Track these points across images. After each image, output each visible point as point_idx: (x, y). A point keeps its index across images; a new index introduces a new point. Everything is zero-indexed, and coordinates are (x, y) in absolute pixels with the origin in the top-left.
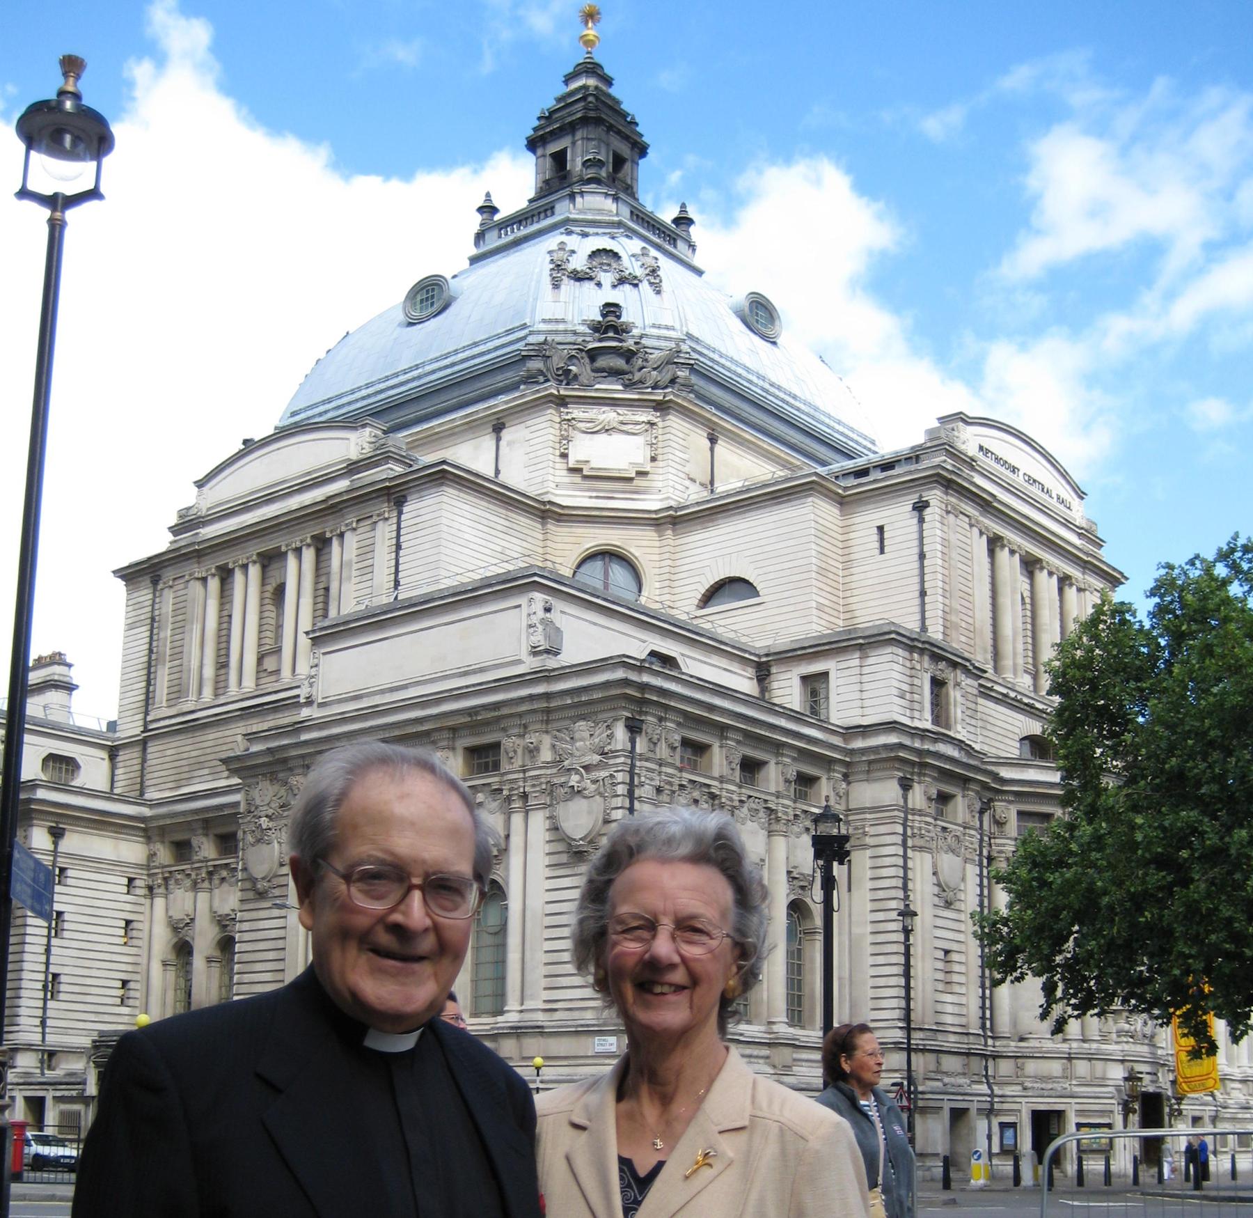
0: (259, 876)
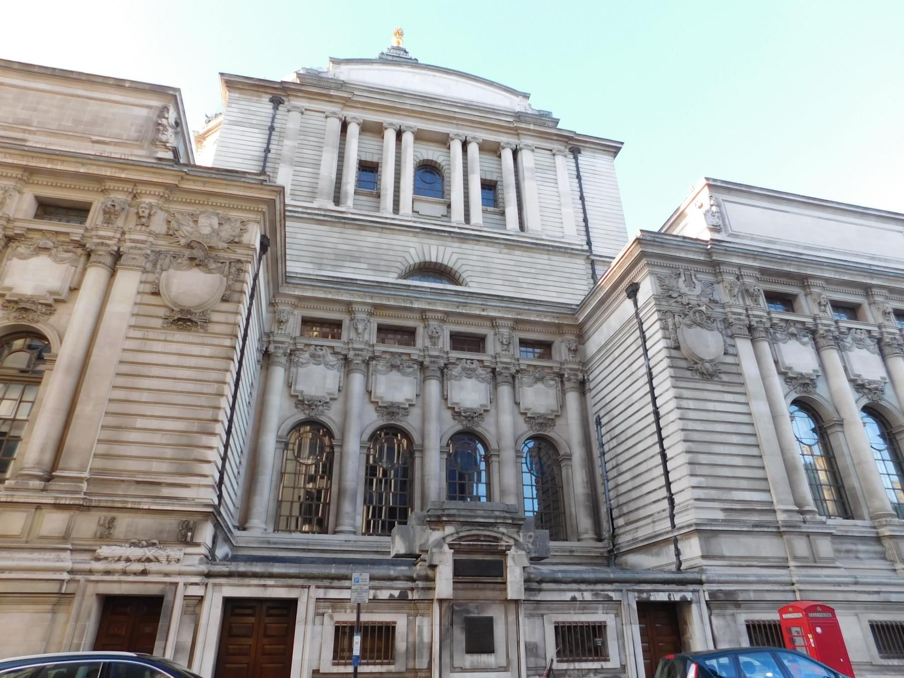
0: (707, 358)
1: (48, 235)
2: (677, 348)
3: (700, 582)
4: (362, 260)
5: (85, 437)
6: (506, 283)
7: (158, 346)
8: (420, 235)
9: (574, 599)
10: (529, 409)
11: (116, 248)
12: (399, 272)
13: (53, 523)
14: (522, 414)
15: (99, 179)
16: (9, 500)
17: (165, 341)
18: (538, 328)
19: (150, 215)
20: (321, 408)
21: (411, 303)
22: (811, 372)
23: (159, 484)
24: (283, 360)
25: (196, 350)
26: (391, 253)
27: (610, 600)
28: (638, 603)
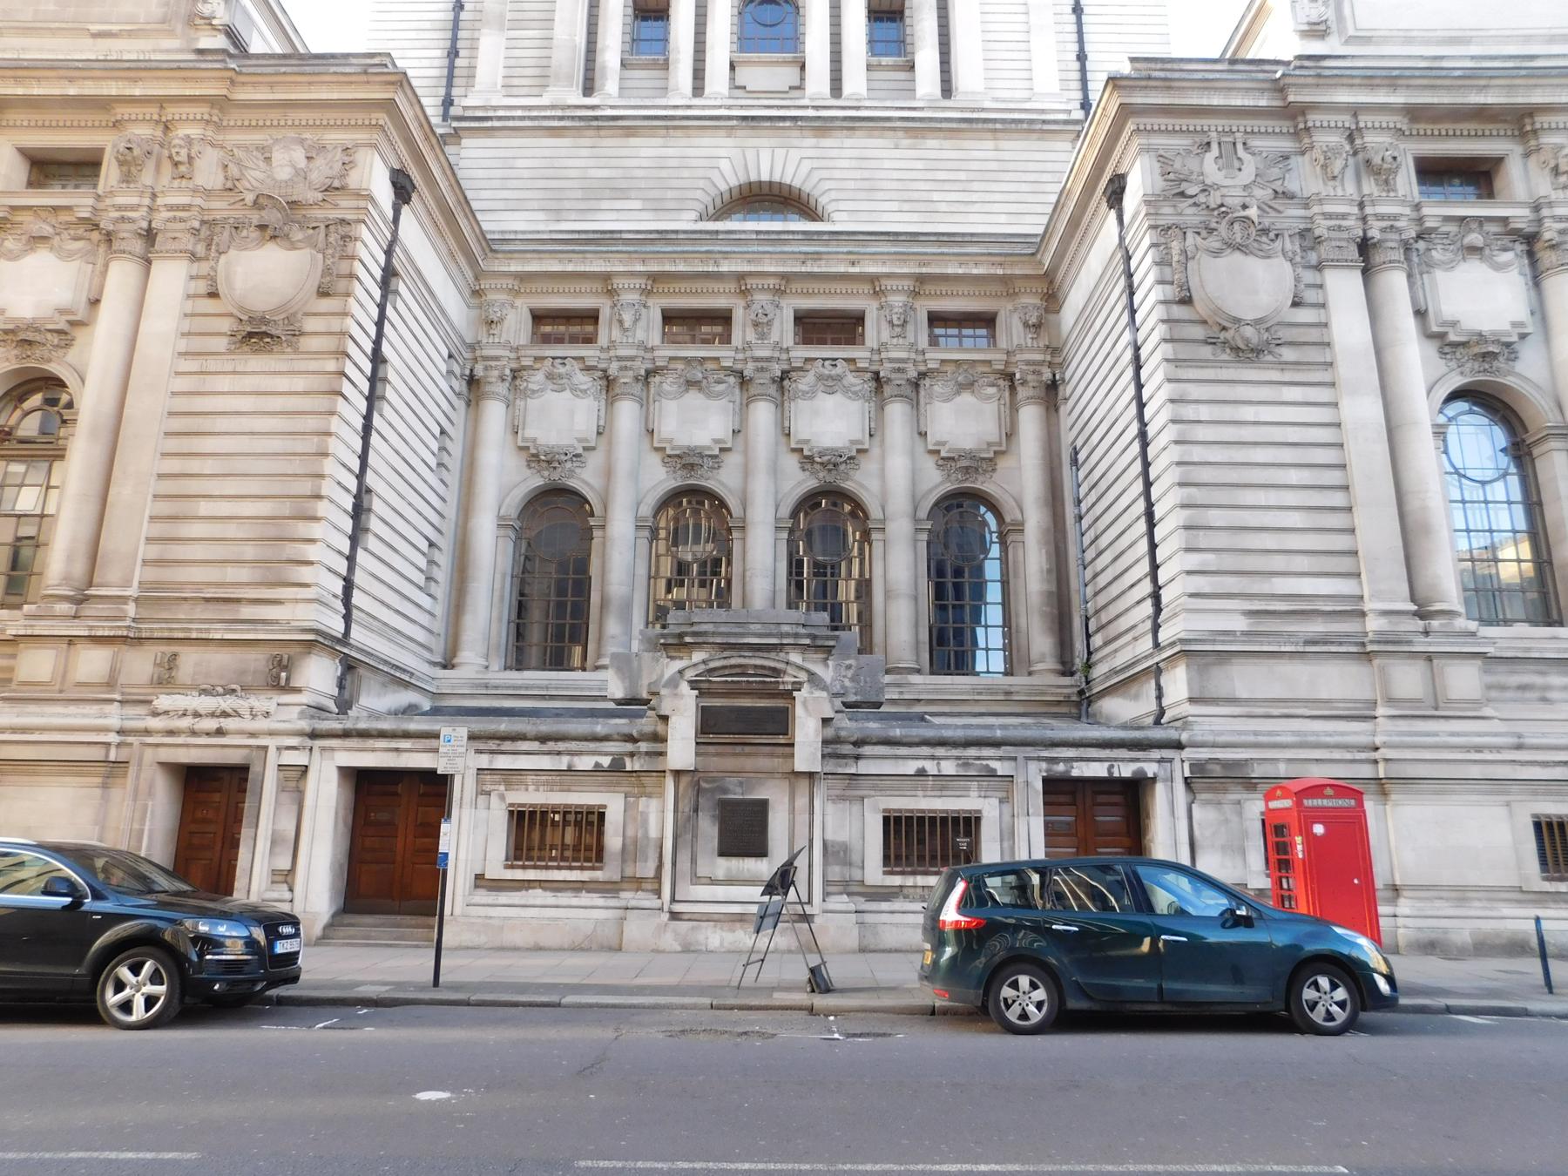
0: (1249, 316)
1: (43, 214)
2: (1186, 301)
3: (1179, 746)
4: (633, 194)
5: (129, 536)
6: (906, 207)
7: (224, 383)
8: (739, 133)
9: (921, 773)
10: (943, 444)
11: (145, 225)
12: (700, 207)
13: (92, 663)
14: (931, 452)
15: (102, 104)
16: (29, 632)
17: (234, 373)
18: (964, 288)
19: (190, 158)
20: (569, 465)
21: (716, 263)
22: (1507, 327)
23: (238, 601)
24: (502, 388)
25: (282, 383)
26: (686, 173)
27: (992, 774)
28: (1046, 781)
